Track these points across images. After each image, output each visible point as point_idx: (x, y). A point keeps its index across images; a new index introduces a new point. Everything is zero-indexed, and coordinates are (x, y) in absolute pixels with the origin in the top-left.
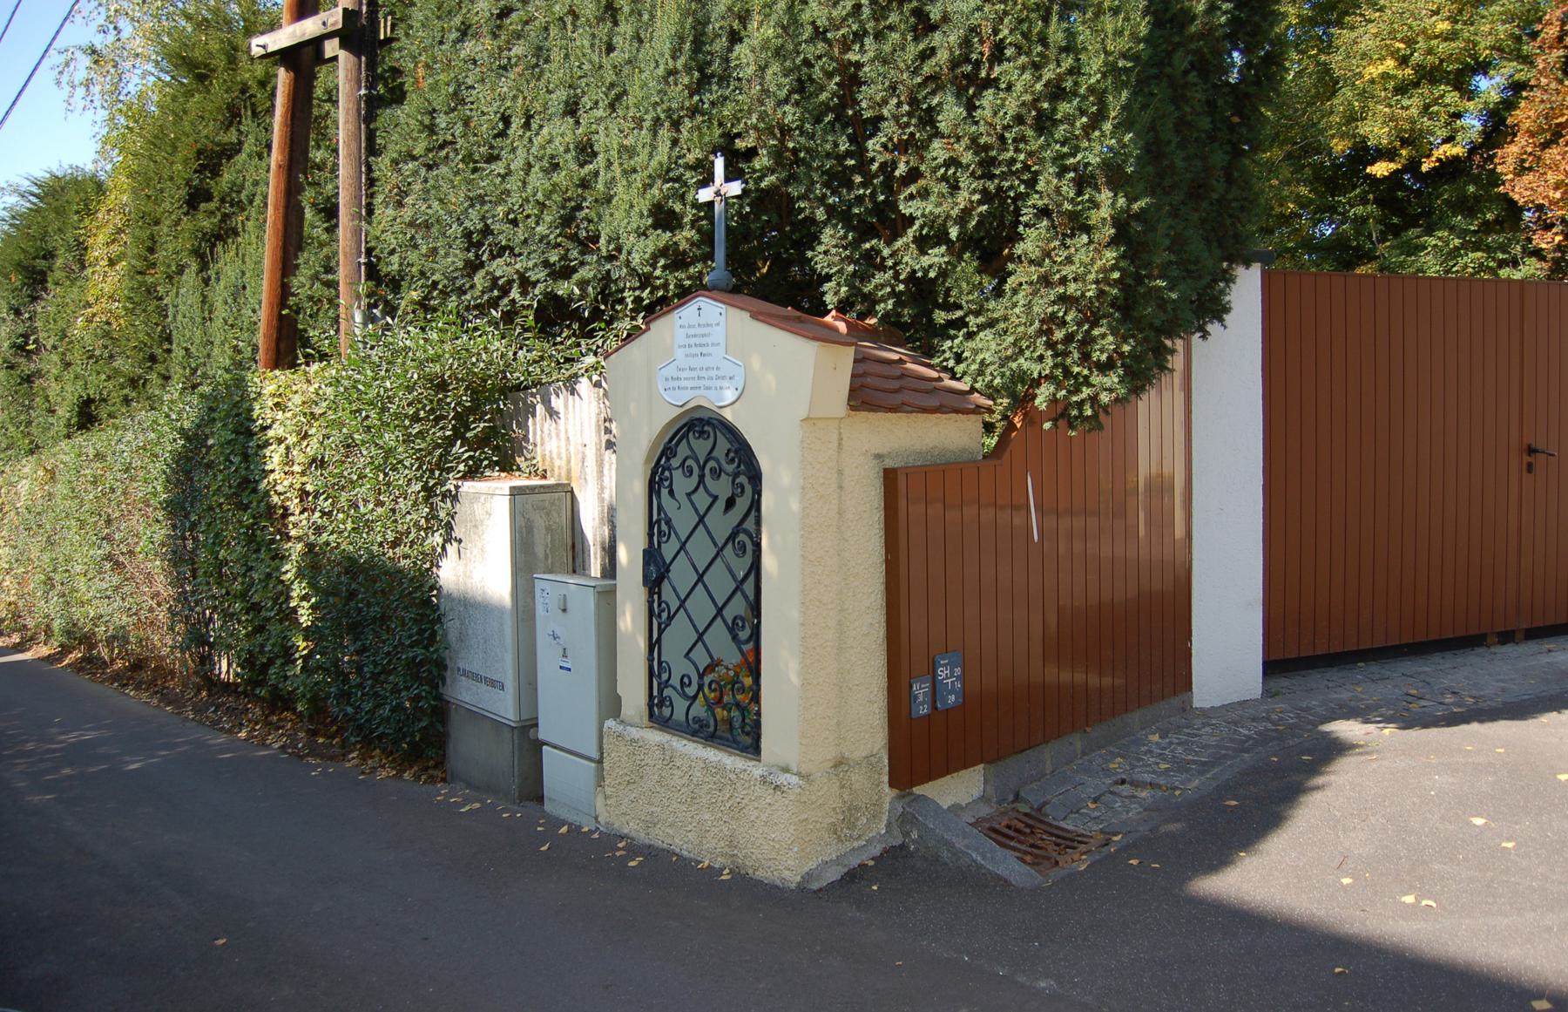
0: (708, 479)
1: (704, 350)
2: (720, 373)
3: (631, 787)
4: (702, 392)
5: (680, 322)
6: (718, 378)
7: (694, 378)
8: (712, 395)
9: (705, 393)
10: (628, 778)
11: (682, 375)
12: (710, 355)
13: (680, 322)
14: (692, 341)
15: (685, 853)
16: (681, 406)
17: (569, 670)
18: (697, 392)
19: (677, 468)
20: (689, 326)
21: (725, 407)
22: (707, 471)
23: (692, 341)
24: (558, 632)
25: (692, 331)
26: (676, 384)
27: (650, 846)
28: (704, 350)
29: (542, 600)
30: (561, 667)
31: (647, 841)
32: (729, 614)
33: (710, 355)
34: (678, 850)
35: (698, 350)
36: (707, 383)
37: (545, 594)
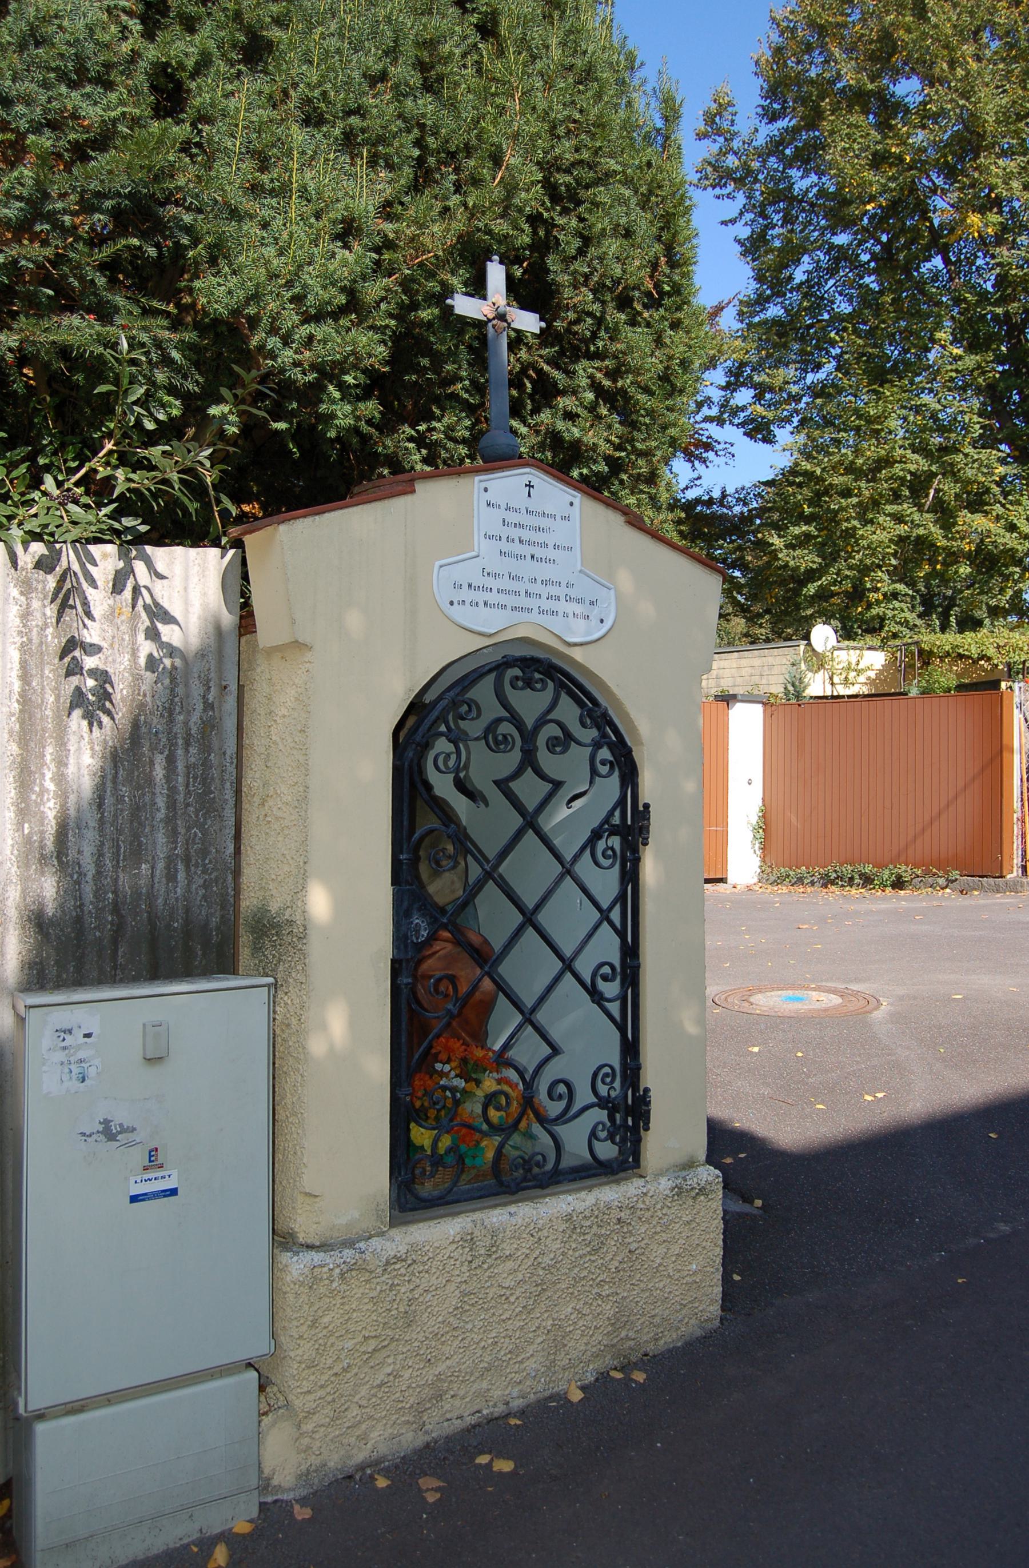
0: (543, 756)
1: (539, 552)
2: (573, 593)
3: (380, 1356)
4: (535, 617)
5: (487, 496)
6: (569, 599)
7: (517, 593)
8: (556, 625)
9: (543, 619)
10: (372, 1344)
11: (490, 582)
12: (548, 561)
13: (487, 496)
14: (515, 533)
15: (517, 1404)
16: (491, 635)
17: (174, 1192)
18: (525, 616)
19: (477, 739)
20: (508, 509)
21: (575, 645)
22: (541, 741)
23: (515, 533)
24: (121, 1116)
25: (512, 517)
26: (480, 597)
27: (427, 1446)
28: (539, 552)
29: (60, 1056)
30: (134, 1199)
31: (421, 1440)
32: (585, 967)
33: (548, 561)
34: (500, 1409)
35: (528, 550)
36: (546, 605)
37: (77, 1038)
